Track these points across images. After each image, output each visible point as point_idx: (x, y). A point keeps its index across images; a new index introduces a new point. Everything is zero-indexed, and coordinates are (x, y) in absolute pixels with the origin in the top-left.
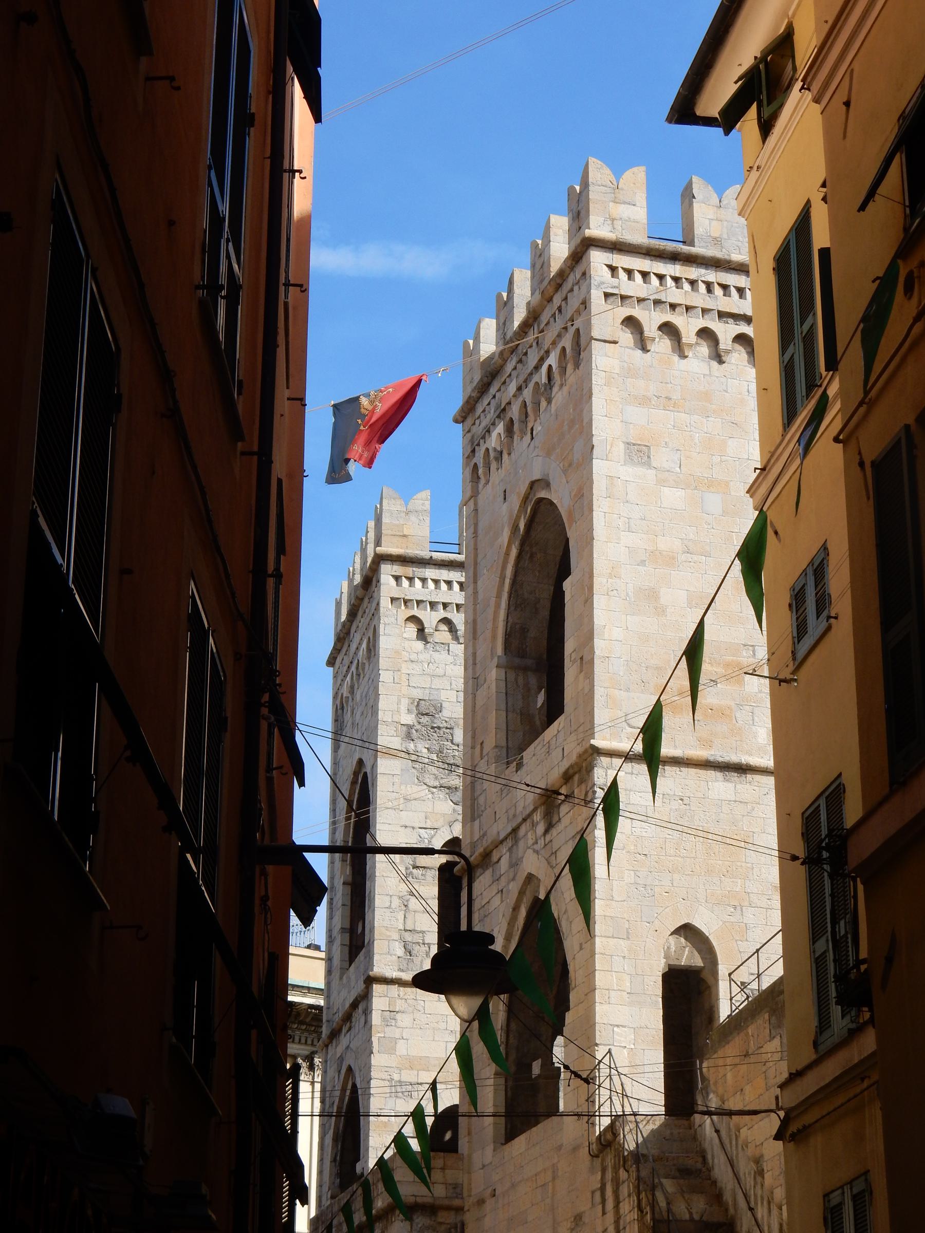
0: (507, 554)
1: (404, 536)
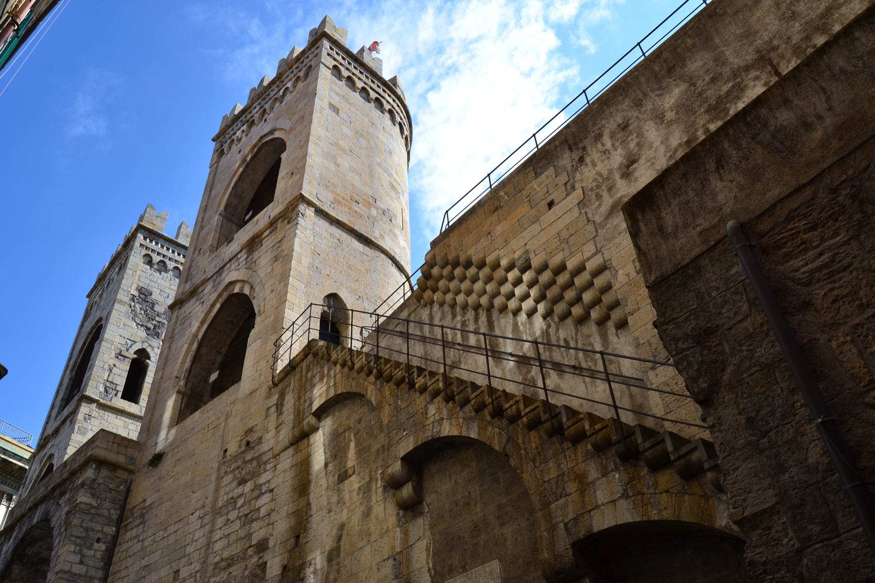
0: (236, 172)
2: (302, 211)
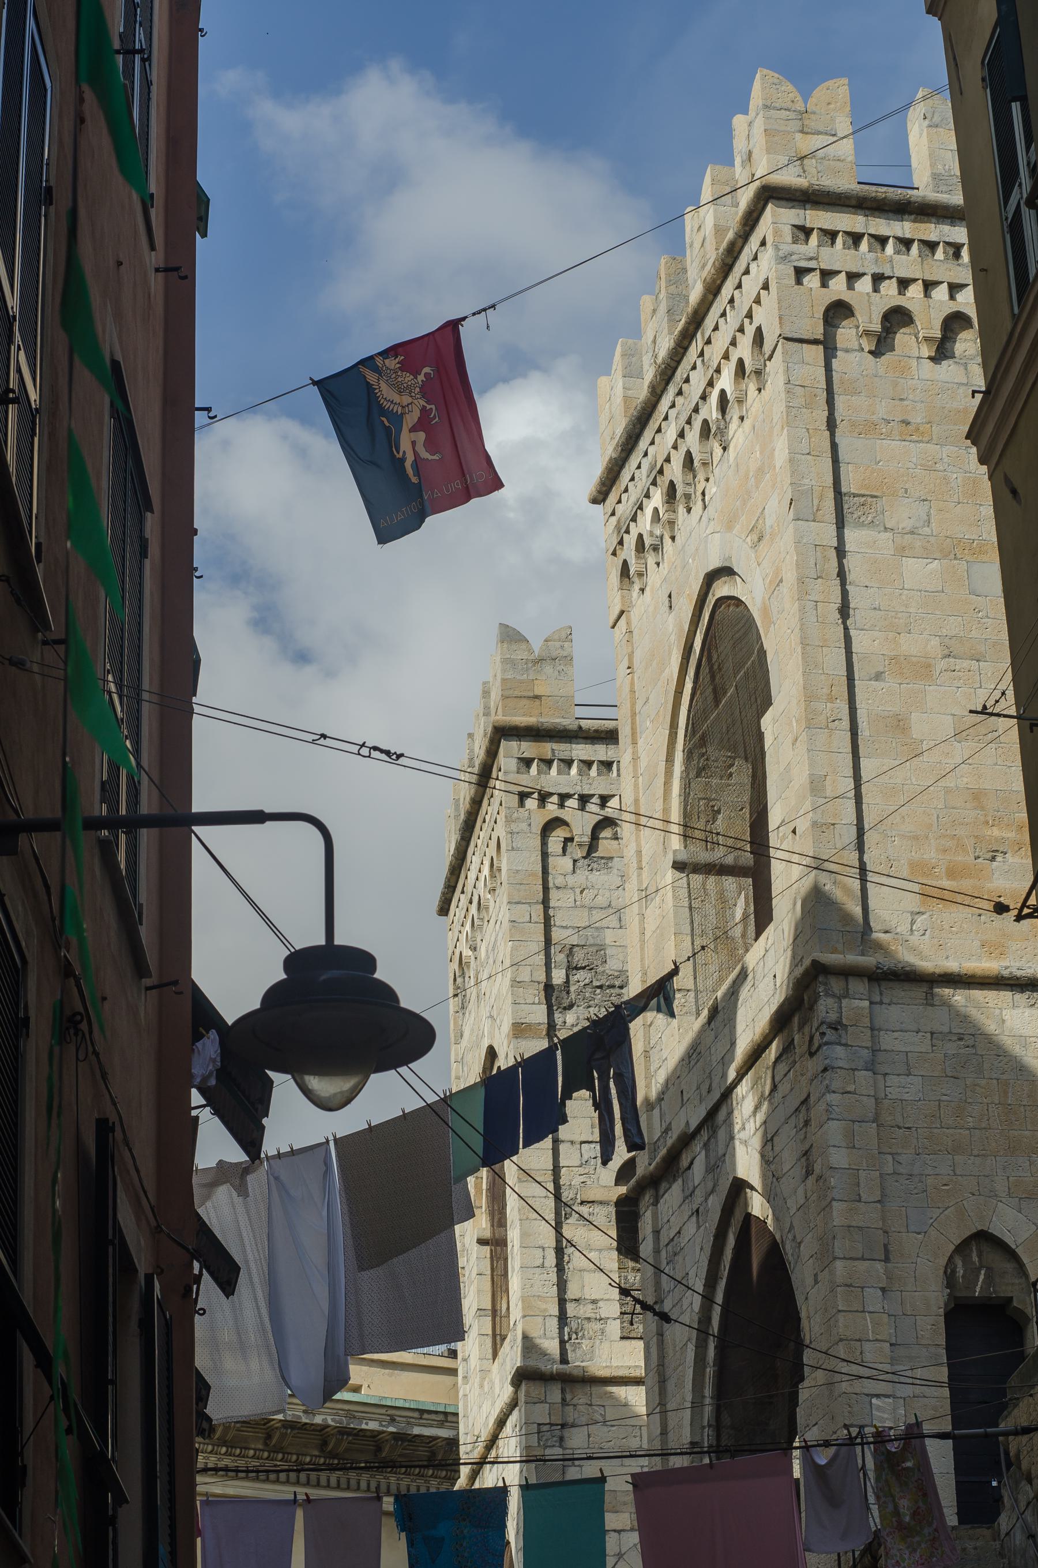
1: (537, 697)
2: (833, 1017)
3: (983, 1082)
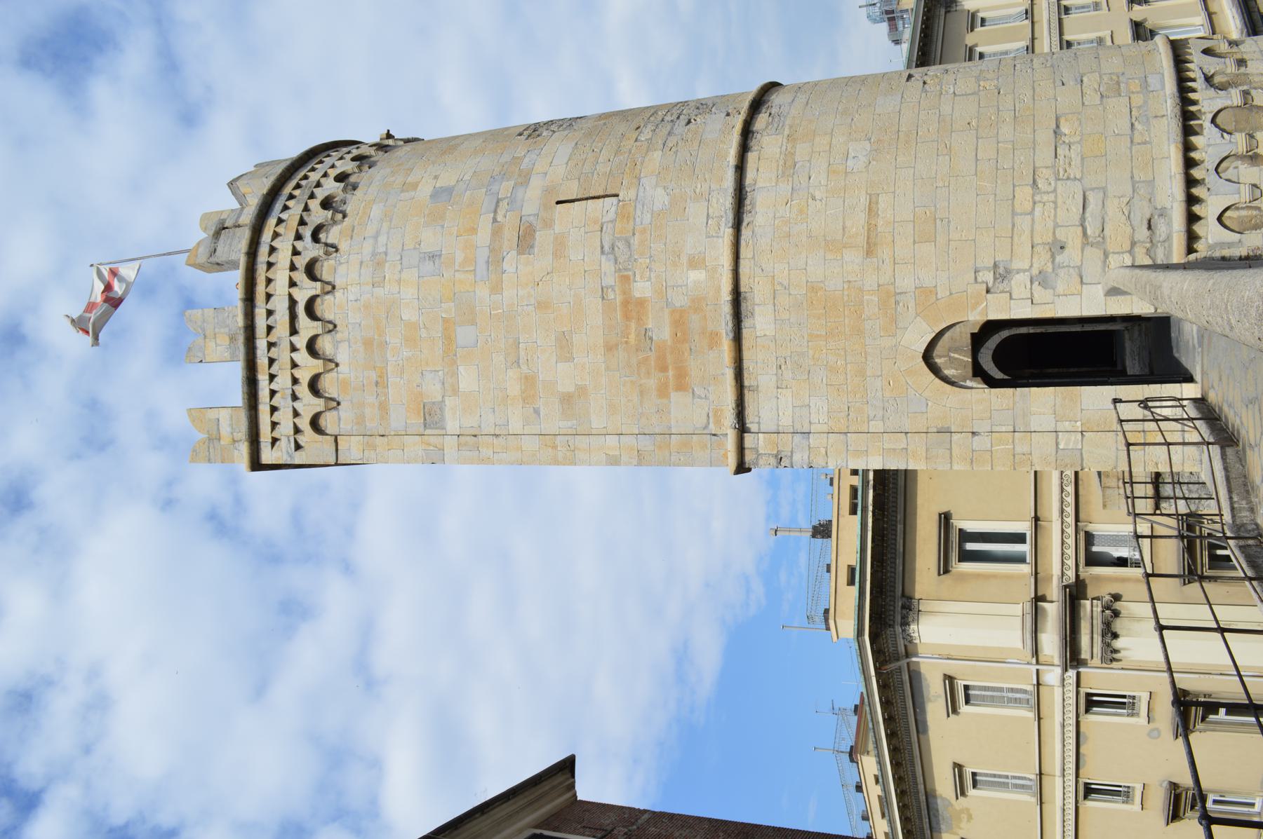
3: (811, 352)
